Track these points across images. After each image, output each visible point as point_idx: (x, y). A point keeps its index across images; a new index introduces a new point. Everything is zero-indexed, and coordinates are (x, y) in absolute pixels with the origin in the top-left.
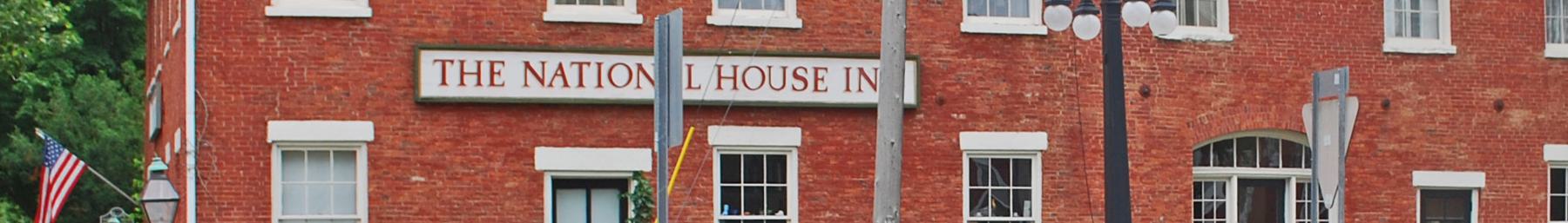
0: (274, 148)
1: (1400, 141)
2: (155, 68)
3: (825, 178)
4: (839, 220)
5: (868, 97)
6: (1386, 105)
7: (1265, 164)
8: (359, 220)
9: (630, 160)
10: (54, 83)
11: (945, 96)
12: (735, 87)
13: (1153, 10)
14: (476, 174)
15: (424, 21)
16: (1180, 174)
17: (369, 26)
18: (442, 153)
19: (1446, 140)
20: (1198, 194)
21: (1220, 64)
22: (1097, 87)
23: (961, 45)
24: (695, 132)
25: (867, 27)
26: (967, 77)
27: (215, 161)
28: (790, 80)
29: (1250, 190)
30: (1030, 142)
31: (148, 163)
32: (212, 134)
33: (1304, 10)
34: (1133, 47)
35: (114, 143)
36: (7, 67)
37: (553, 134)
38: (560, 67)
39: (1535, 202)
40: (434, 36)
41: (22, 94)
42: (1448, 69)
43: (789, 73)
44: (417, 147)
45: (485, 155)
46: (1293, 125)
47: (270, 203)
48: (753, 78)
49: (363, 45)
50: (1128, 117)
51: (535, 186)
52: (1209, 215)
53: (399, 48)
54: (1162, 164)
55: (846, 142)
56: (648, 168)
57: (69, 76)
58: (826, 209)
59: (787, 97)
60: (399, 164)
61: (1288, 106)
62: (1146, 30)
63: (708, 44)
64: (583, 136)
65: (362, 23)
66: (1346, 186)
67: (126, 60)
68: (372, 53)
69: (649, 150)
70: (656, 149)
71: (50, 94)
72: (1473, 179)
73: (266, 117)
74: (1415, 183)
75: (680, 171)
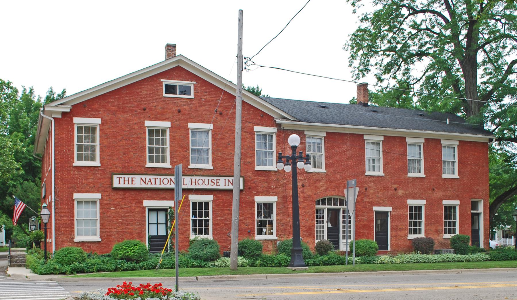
0: (75, 200)
1: (370, 199)
2: (44, 180)
3: (219, 208)
4: (223, 219)
5: (231, 187)
6: (366, 189)
7: (334, 205)
8: (97, 219)
9: (169, 204)
10: (17, 183)
11: (250, 187)
12: (196, 185)
13: (305, 164)
14: (128, 207)
15: (114, 167)
16: (312, 207)
17: (100, 168)
18: (119, 202)
19: (382, 198)
20: (317, 213)
21: (323, 178)
22: (290, 184)
23: (255, 173)
24: (185, 196)
25: (230, 169)
26: (256, 182)
27: (60, 204)
28: (210, 183)
29: (330, 212)
30: (273, 199)
31: (42, 204)
32: (59, 197)
33: (345, 164)
34: (300, 174)
35: (33, 199)
36: (5, 179)
37: (148, 197)
38: (150, 179)
39: (405, 215)
40: (117, 171)
41: (9, 186)
42: (382, 180)
43: (210, 181)
44: (112, 200)
45: (130, 202)
46: (342, 195)
47: (74, 215)
48: (201, 182)
49: (98, 173)
50: (299, 192)
51: (143, 210)
52: (320, 218)
53: (108, 174)
54: (307, 205)
55: (225, 199)
56: (173, 206)
57: (21, 181)
58: (219, 217)
59: (209, 187)
60: (108, 205)
61: (341, 189)
62: (303, 170)
63: (189, 173)
64: (156, 197)
65: (98, 168)
66: (356, 210)
67: (36, 177)
68: (101, 175)
69: (173, 201)
70: (175, 201)
71: (16, 186)
72: (389, 209)
73: (73, 192)
74: (374, 210)
75: (181, 207)
